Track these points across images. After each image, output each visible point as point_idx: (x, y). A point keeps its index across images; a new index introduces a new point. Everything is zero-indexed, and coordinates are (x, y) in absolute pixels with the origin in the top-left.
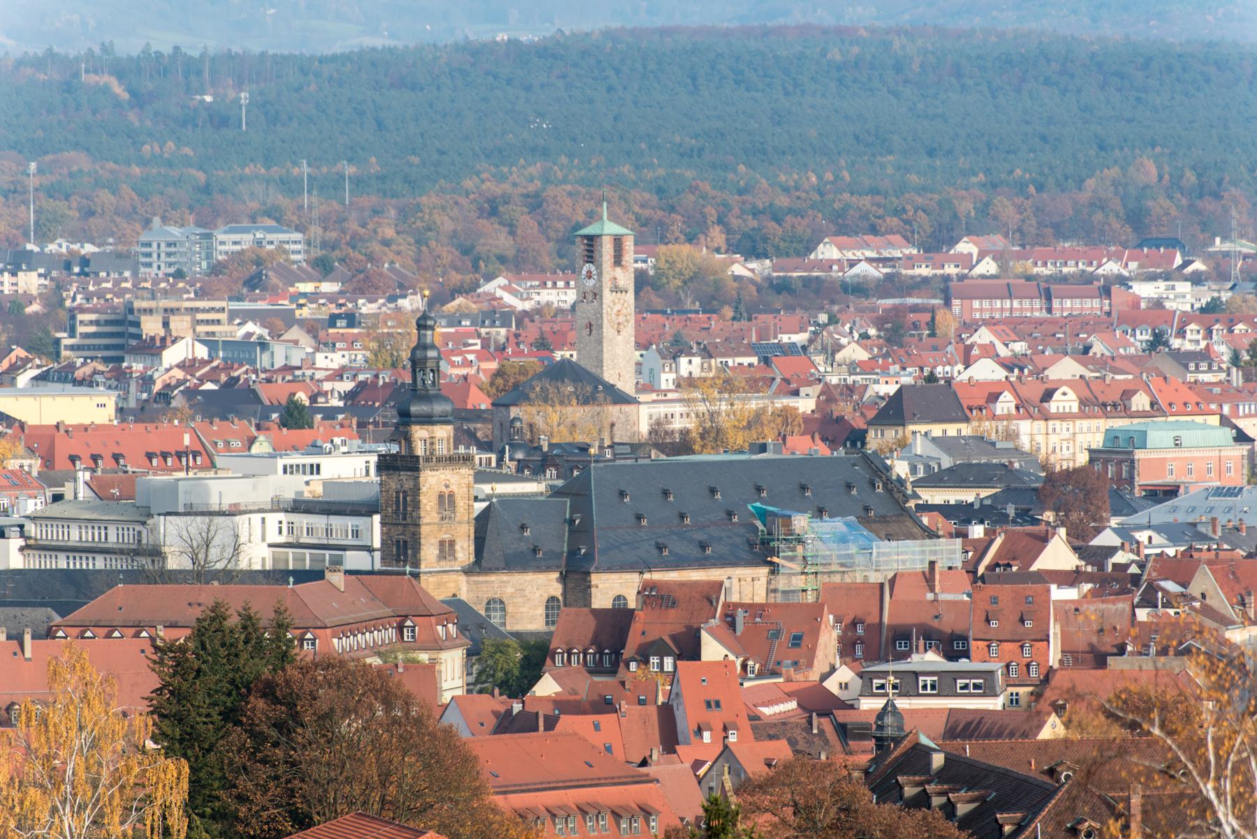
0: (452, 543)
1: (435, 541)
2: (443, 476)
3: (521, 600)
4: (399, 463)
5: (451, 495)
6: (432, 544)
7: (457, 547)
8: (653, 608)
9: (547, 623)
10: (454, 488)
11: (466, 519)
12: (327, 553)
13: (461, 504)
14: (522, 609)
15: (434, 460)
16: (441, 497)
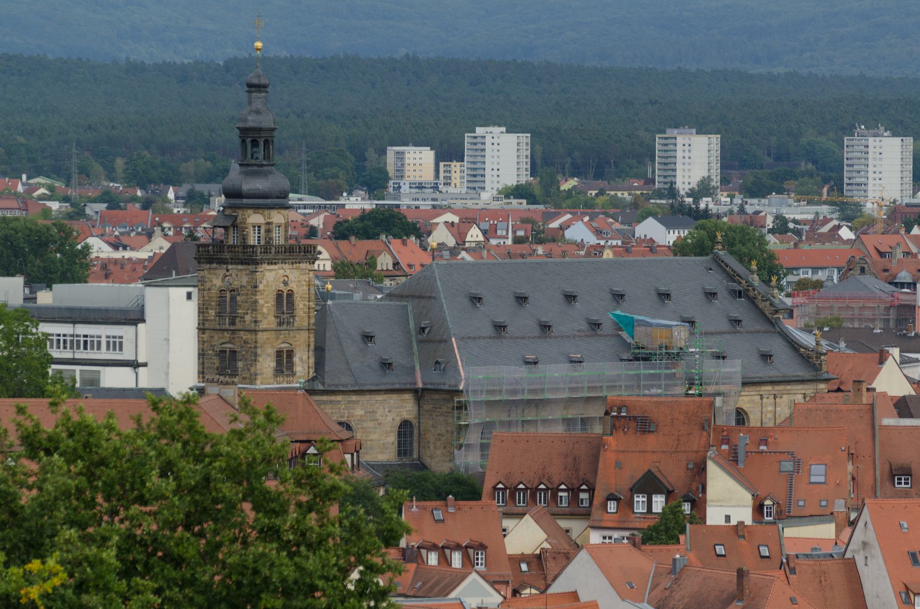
0: (290, 354)
1: (271, 351)
2: (281, 272)
3: (371, 424)
4: (227, 255)
5: (290, 294)
6: (269, 355)
7: (296, 359)
8: (625, 433)
9: (399, 454)
10: (293, 286)
11: (305, 324)
12: (78, 368)
13: (301, 306)
14: (373, 436)
15: (273, 250)
16: (279, 296)
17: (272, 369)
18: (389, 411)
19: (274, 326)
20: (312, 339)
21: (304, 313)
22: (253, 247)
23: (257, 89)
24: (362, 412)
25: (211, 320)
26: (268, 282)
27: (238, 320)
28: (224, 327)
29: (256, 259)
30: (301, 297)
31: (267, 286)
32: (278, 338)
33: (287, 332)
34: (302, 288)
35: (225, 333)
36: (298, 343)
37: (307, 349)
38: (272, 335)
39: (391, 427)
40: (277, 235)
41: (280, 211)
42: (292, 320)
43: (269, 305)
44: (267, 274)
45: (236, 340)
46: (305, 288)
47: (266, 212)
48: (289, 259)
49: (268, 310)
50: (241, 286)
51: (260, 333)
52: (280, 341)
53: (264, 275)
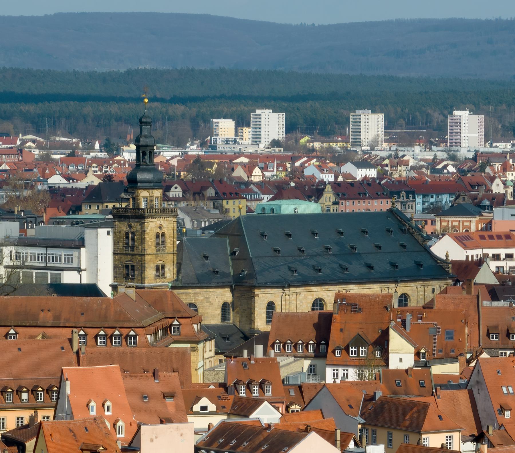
0: (163, 267)
1: (153, 266)
3: (207, 304)
6: (152, 268)
7: (166, 270)
10: (165, 230)
11: (172, 250)
14: (208, 311)
17: (154, 275)
18: (217, 297)
19: (155, 252)
20: (175, 259)
21: (171, 244)
22: (143, 209)
23: (145, 124)
24: (202, 298)
25: (121, 249)
26: (151, 228)
27: (135, 248)
28: (127, 252)
29: (145, 216)
30: (169, 236)
31: (151, 230)
32: (156, 258)
33: (162, 255)
34: (170, 231)
35: (128, 256)
36: (168, 261)
37: (173, 263)
38: (153, 257)
39: (218, 306)
40: (156, 203)
41: (158, 190)
42: (164, 248)
43: (152, 240)
44: (151, 224)
45: (134, 259)
46: (171, 231)
47: (150, 191)
48: (163, 216)
49: (152, 243)
50: (137, 231)
51: (147, 256)
52: (158, 260)
53: (149, 225)
